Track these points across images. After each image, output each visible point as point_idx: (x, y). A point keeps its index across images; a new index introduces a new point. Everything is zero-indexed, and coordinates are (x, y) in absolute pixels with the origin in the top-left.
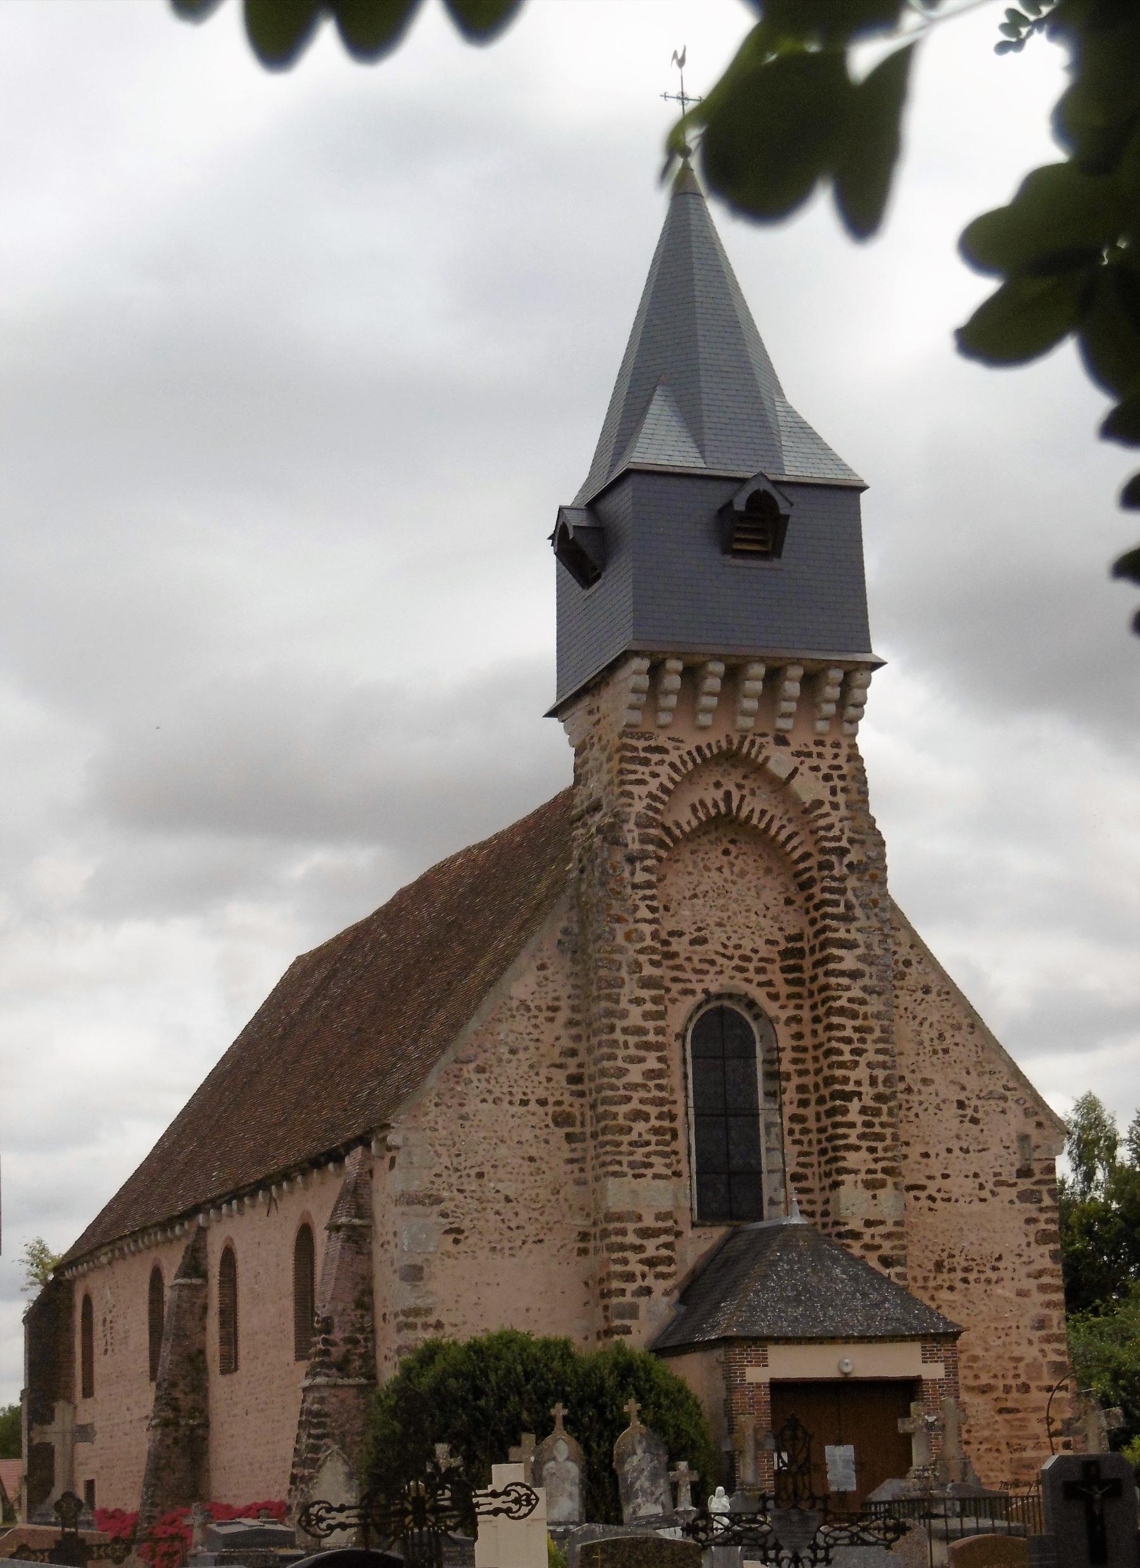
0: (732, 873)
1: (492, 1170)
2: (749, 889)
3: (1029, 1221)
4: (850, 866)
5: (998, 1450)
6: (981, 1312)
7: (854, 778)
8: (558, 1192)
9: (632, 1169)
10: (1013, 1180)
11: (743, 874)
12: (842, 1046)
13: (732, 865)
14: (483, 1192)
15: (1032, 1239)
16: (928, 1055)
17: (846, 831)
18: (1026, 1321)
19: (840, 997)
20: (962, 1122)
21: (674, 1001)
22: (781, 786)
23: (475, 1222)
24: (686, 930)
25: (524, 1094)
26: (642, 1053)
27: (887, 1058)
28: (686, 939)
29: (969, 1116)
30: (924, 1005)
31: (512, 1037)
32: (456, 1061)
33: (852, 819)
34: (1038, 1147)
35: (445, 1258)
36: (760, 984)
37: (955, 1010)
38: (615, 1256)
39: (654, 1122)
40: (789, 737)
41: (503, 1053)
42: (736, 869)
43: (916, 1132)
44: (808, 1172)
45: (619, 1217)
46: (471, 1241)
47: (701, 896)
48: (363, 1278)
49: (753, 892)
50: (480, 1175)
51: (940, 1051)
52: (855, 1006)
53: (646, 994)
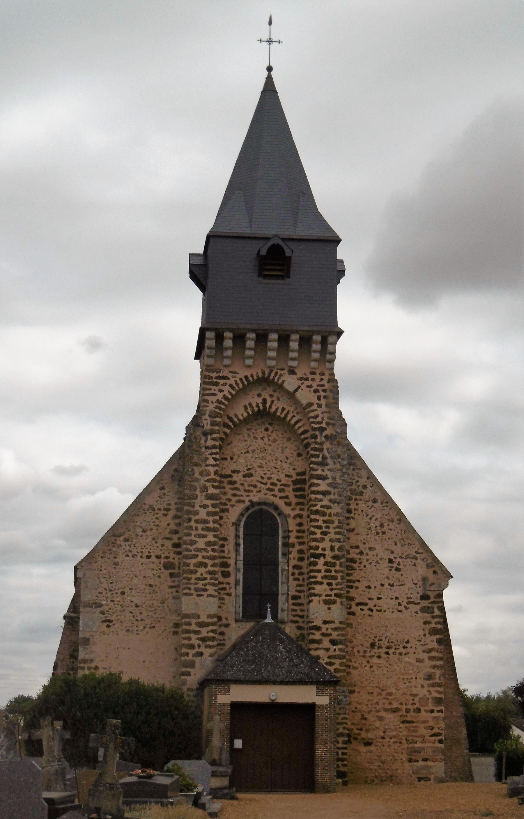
0: (269, 440)
1: (129, 591)
2: (278, 449)
3: (425, 623)
4: (326, 437)
5: (400, 743)
6: (396, 669)
7: (331, 391)
8: (164, 603)
9: (196, 591)
10: (419, 601)
11: (275, 441)
12: (316, 530)
13: (269, 436)
14: (124, 602)
15: (427, 632)
16: (373, 535)
17: (325, 419)
18: (421, 675)
19: (316, 505)
20: (390, 570)
21: (233, 506)
22: (292, 396)
23: (119, 617)
24: (241, 469)
25: (149, 552)
26: (205, 533)
27: (340, 537)
28: (241, 475)
29: (395, 567)
30: (373, 509)
31: (144, 524)
32: (113, 536)
33: (329, 412)
34: (433, 584)
35: (102, 634)
36: (281, 498)
37: (390, 512)
38: (184, 636)
39: (210, 568)
40: (296, 370)
41: (138, 532)
42: (271, 438)
43: (364, 575)
44: (302, 595)
45: (187, 616)
46: (116, 626)
47: (251, 452)
48: (75, 643)
49: (280, 450)
50: (123, 593)
51: (381, 533)
52: (325, 510)
53: (209, 502)
